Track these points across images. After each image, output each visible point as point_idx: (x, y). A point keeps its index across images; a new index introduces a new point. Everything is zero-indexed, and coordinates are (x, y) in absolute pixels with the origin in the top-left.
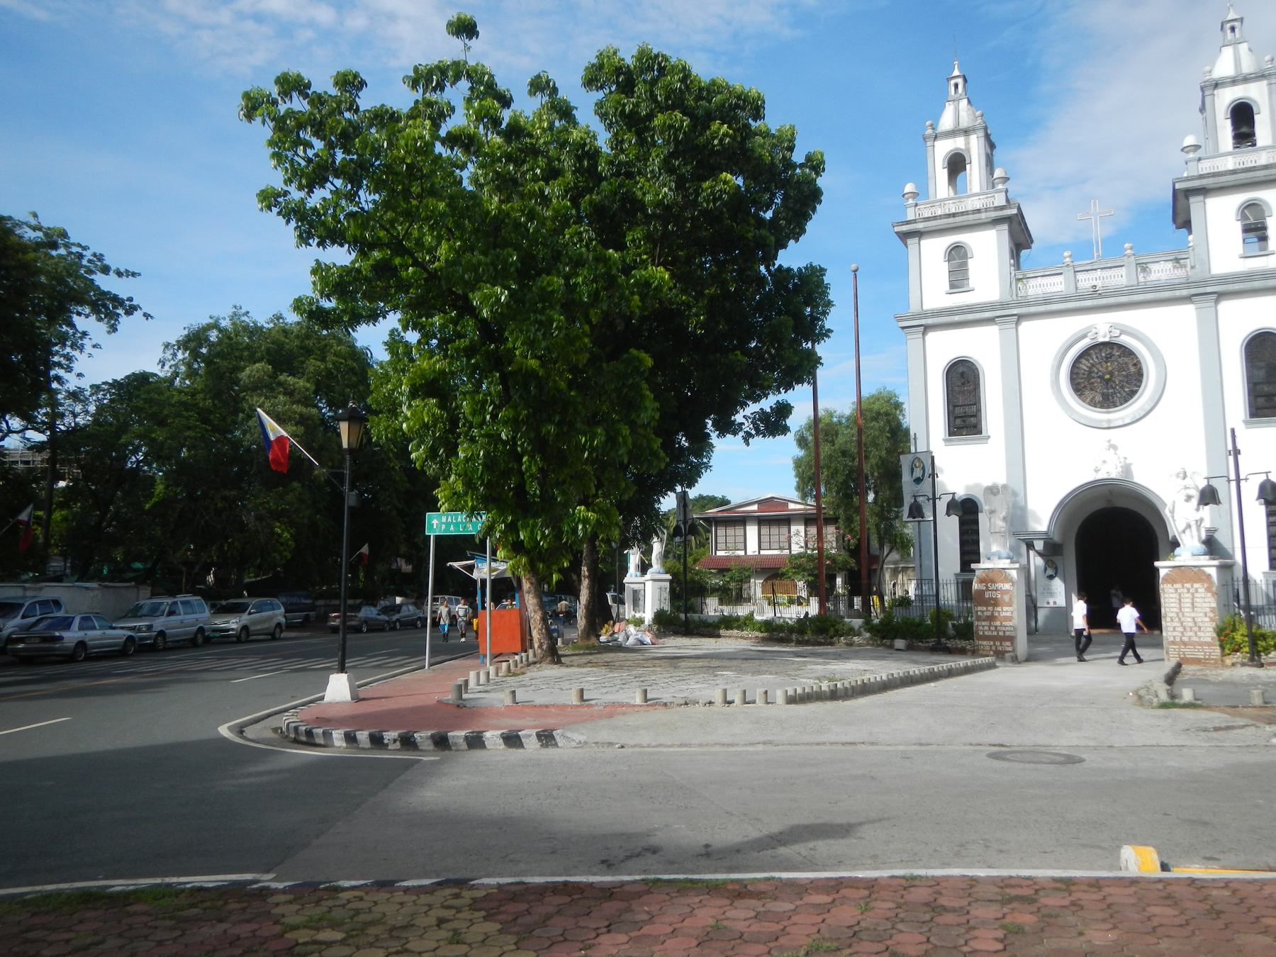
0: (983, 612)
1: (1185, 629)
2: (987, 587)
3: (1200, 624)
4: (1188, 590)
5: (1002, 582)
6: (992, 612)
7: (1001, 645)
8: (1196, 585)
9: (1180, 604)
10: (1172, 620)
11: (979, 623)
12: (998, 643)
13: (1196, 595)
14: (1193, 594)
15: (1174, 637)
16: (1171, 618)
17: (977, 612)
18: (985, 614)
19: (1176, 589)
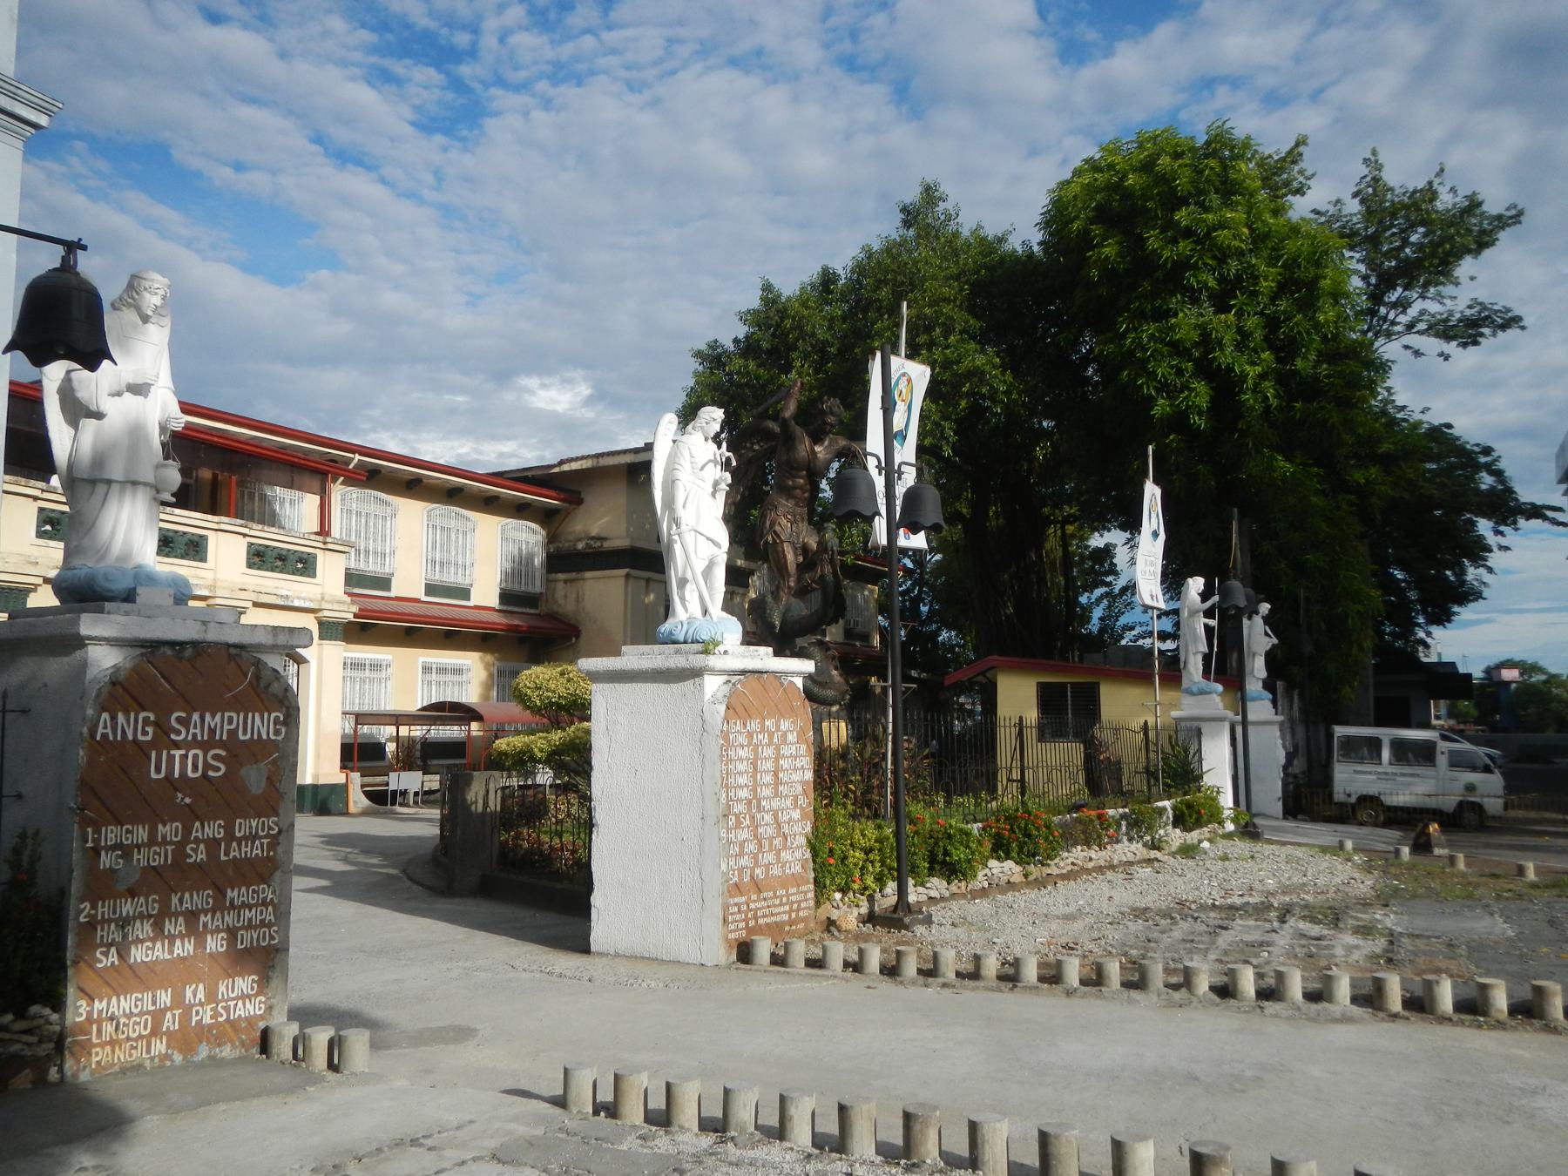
0: (126, 851)
1: (760, 845)
2: (162, 728)
3: (786, 829)
4: (771, 735)
5: (241, 704)
6: (180, 847)
7: (212, 997)
8: (785, 725)
9: (754, 777)
10: (738, 825)
11: (103, 910)
12: (195, 993)
13: (785, 751)
14: (778, 749)
15: (741, 870)
16: (737, 817)
17: (96, 851)
18: (140, 858)
19: (750, 735)
